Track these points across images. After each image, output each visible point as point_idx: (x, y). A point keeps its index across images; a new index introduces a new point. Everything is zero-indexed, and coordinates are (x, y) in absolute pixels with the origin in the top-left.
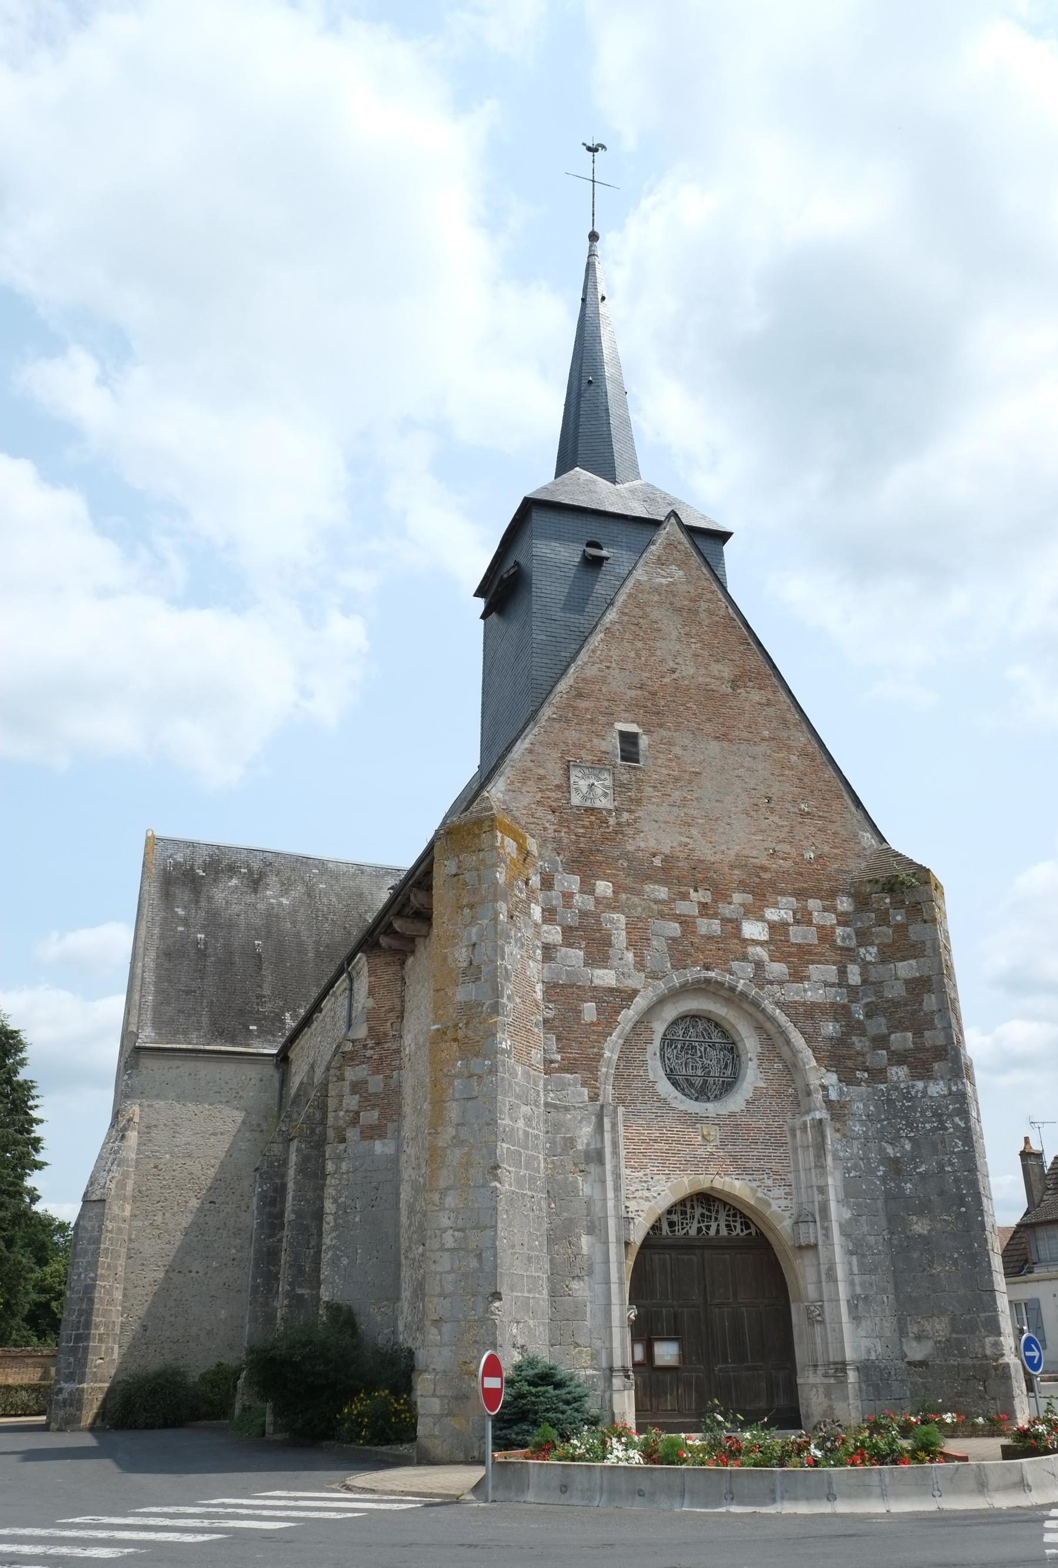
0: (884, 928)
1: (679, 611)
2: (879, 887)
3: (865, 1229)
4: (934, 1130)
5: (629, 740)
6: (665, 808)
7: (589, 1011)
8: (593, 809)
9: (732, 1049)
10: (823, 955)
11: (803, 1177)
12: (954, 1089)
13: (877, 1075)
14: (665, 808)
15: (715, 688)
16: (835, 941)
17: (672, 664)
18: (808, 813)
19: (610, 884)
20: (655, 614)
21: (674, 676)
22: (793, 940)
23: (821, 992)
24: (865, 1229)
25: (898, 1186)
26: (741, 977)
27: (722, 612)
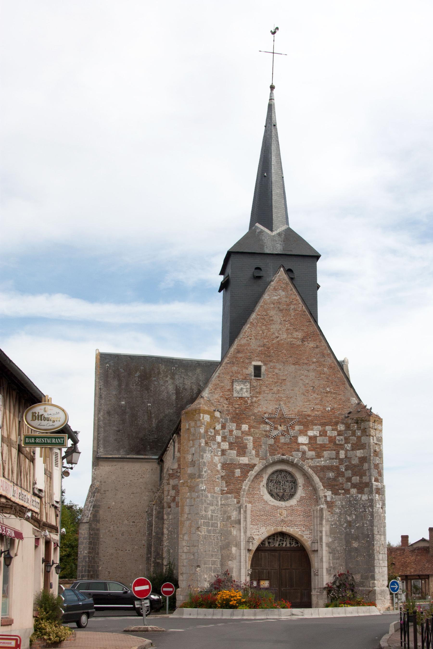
0: (353, 437)
1: (281, 310)
2: (354, 421)
3: (337, 545)
4: (362, 512)
5: (257, 369)
6: (270, 395)
7: (238, 472)
8: (242, 397)
9: (294, 482)
10: (330, 447)
11: (316, 527)
12: (370, 498)
13: (347, 491)
14: (270, 395)
15: (295, 343)
16: (336, 442)
17: (277, 335)
18: (329, 392)
19: (247, 426)
20: (272, 313)
21: (278, 340)
22: (318, 442)
23: (328, 461)
24: (337, 545)
25: (350, 530)
26: (296, 457)
27: (300, 309)
